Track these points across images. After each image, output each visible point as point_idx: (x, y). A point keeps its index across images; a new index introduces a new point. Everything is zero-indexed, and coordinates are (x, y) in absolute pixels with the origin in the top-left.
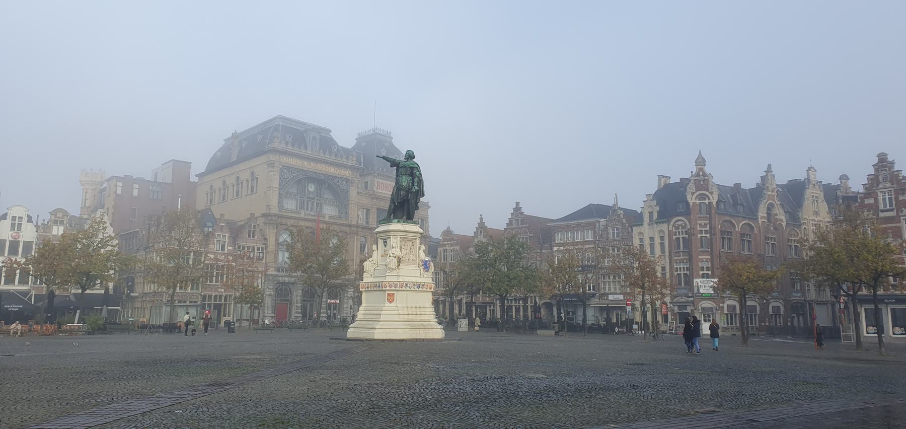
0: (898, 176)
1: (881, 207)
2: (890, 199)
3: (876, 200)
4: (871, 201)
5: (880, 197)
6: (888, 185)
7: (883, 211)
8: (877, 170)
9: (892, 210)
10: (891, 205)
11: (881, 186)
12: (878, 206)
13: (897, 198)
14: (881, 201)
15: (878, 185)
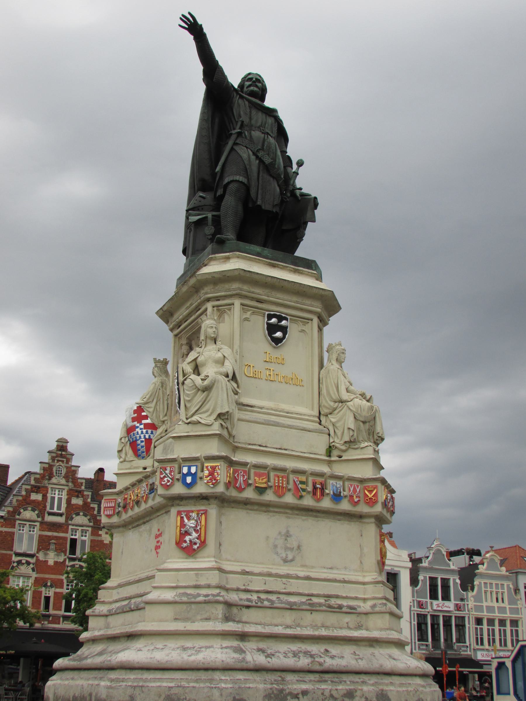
0: (75, 472)
1: (48, 509)
2: (60, 499)
3: (45, 497)
4: (36, 497)
5: (49, 495)
6: (63, 481)
7: (50, 514)
8: (53, 459)
9: (61, 515)
10: (59, 508)
11: (54, 480)
12: (45, 507)
13: (69, 501)
14: (49, 500)
15: (50, 478)
